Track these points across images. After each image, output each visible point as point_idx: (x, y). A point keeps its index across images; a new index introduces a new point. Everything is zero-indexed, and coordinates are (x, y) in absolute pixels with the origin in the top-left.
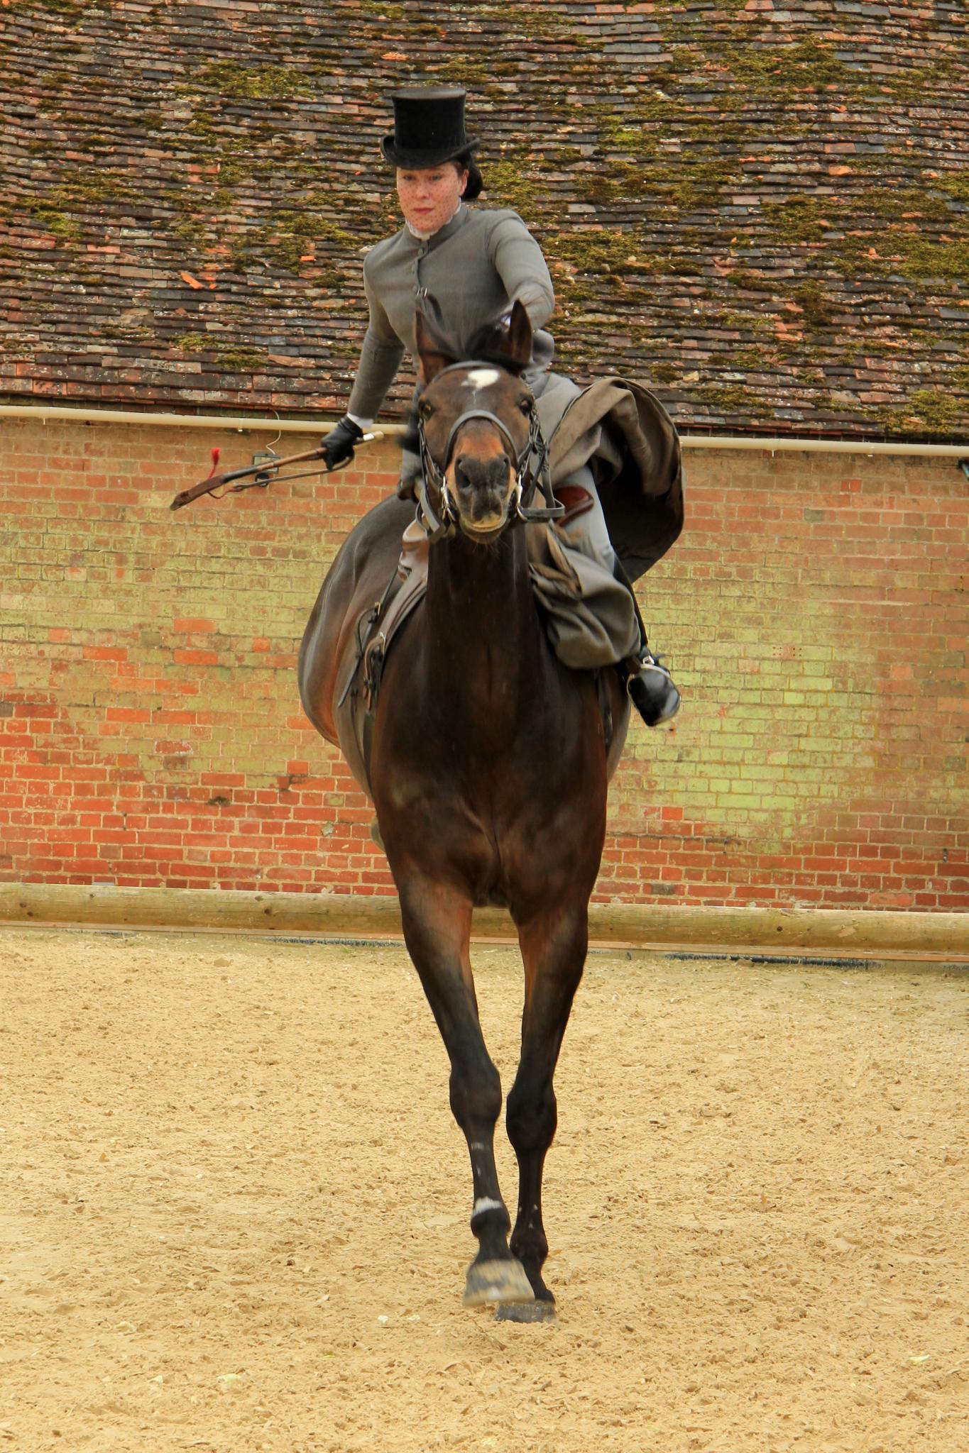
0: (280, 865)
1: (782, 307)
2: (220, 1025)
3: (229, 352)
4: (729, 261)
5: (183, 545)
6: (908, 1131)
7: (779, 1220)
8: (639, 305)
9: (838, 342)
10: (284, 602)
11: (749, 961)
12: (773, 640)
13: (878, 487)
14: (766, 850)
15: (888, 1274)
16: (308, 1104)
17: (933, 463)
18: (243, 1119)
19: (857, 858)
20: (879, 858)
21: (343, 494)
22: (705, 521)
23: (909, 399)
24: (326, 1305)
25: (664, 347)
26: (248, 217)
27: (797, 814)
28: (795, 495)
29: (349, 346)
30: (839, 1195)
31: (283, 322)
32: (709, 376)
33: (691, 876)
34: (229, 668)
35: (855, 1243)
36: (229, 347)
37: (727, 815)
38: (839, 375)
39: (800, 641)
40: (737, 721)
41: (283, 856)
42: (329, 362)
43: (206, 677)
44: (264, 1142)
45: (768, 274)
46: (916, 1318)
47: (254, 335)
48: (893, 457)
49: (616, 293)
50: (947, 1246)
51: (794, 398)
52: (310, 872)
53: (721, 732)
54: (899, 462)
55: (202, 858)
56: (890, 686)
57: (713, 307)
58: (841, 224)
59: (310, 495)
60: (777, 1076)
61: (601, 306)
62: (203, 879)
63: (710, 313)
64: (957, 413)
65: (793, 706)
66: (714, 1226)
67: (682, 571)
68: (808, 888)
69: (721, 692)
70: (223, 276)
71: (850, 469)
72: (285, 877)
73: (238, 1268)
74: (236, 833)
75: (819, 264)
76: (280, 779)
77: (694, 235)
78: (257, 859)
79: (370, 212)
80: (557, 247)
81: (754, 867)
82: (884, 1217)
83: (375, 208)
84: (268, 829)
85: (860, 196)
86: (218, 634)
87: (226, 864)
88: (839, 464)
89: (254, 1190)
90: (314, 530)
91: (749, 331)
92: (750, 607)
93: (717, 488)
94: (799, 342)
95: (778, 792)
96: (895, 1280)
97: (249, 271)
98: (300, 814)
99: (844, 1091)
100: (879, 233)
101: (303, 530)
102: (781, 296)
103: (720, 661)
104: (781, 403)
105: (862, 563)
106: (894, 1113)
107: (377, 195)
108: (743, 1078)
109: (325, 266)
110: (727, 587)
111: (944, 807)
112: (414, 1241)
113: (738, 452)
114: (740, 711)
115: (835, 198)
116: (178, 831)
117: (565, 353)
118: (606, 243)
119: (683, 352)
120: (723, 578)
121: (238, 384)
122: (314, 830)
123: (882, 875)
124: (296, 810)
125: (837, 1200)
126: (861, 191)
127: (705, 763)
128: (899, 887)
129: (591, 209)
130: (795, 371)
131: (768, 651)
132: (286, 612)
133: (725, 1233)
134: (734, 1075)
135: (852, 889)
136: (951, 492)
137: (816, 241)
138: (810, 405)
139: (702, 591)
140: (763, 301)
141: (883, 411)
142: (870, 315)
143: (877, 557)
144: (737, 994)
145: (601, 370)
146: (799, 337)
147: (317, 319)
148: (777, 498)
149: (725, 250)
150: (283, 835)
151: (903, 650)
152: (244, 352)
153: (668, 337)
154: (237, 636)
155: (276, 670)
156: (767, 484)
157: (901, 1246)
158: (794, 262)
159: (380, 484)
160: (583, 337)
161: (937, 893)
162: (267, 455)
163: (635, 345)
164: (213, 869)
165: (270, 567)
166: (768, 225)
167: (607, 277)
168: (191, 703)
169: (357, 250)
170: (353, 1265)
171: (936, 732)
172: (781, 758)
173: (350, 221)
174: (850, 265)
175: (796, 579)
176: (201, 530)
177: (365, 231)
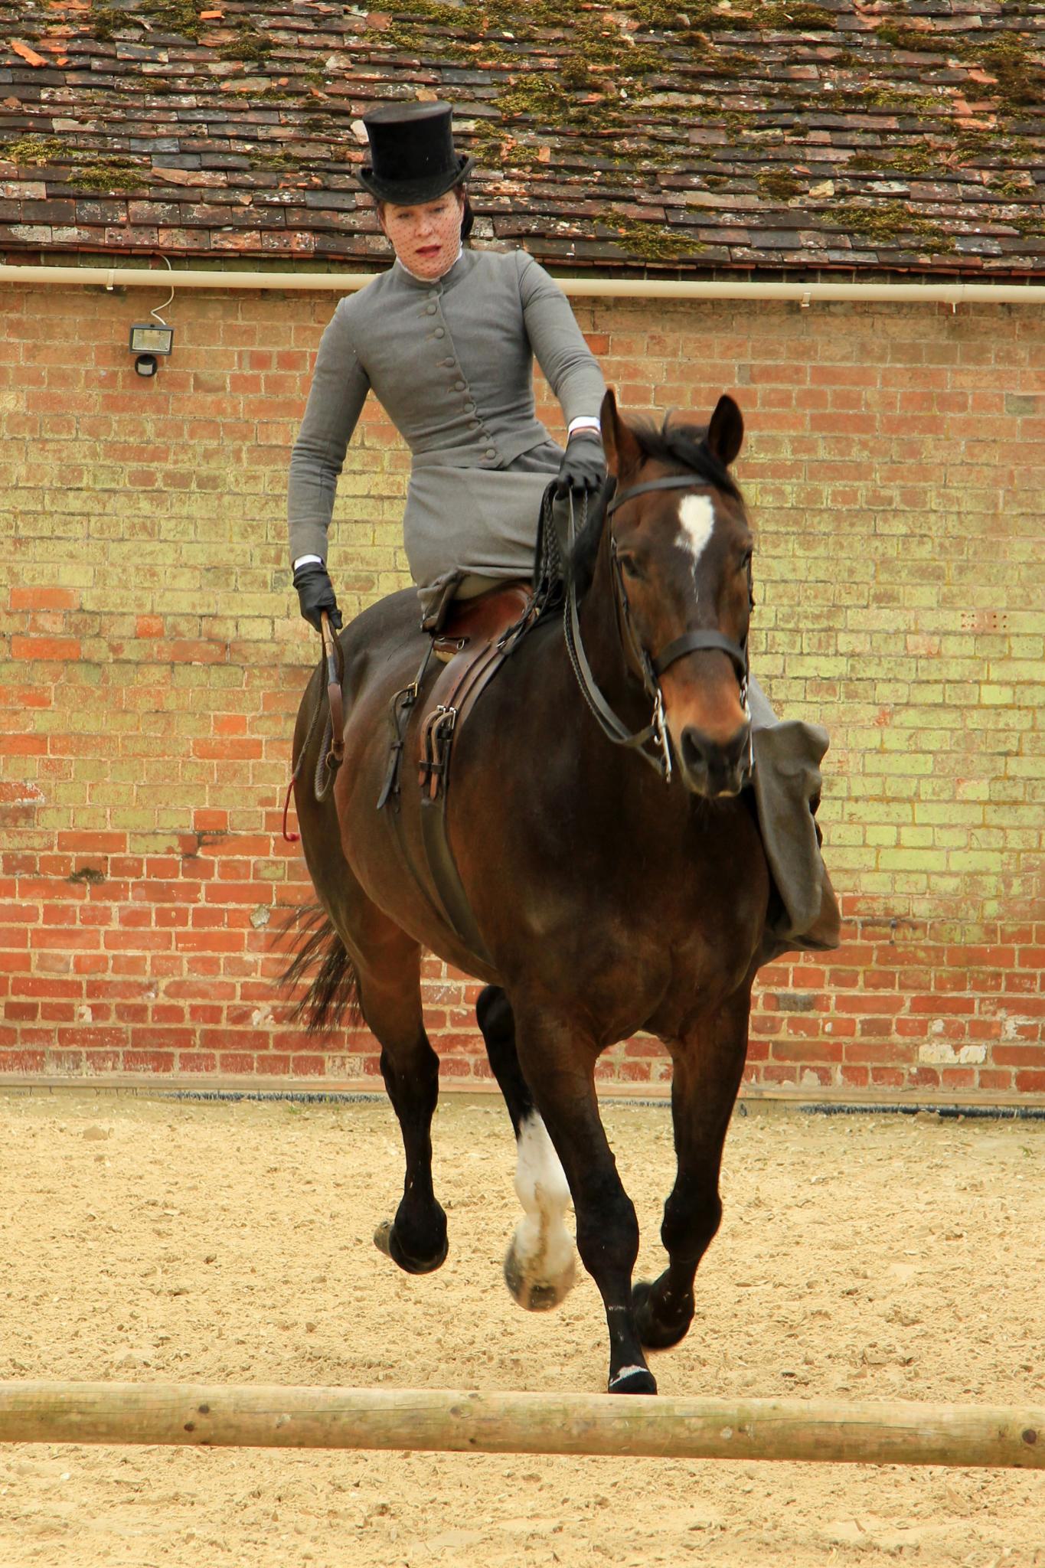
1: (964, 76)
2: (94, 1233)
3: (89, 164)
5: (23, 470)
7: (993, 1529)
8: (737, 79)
10: (183, 560)
11: (935, 1115)
12: (963, 604)
14: (957, 938)
21: (275, 385)
22: (848, 417)
25: (779, 143)
27: (1006, 880)
28: (992, 372)
31: (174, 116)
32: (850, 188)
33: (839, 980)
34: (99, 665)
36: (89, 156)
37: (894, 882)
39: (1004, 604)
40: (909, 732)
41: (191, 961)
42: (249, 178)
43: (62, 679)
45: (941, 25)
47: (130, 137)
49: (700, 60)
51: (985, 219)
52: (234, 986)
53: (881, 751)
55: (61, 966)
57: (854, 79)
59: (224, 388)
60: (984, 1298)
61: (677, 80)
62: (64, 1000)
63: (849, 87)
65: (996, 707)
66: (890, 1541)
67: (814, 496)
68: (1025, 995)
69: (880, 686)
70: (77, 45)
72: (193, 995)
74: (115, 926)
76: (184, 839)
78: (148, 968)
81: (941, 964)
86: (81, 610)
87: (99, 977)
90: (230, 444)
91: (912, 115)
92: (924, 552)
93: (867, 364)
94: (992, 131)
95: (975, 845)
97: (119, 35)
98: (214, 894)
101: (213, 444)
102: (962, 60)
103: (878, 639)
104: (965, 228)
108: (929, 1302)
109: (239, 25)
110: (885, 520)
113: (899, 307)
114: (910, 717)
116: (22, 925)
117: (622, 156)
119: (807, 151)
120: (880, 507)
121: (104, 215)
122: (244, 919)
124: (208, 887)
127: (857, 800)
130: (986, 176)
131: (952, 620)
133: (906, 1551)
134: (915, 1296)
138: (1010, 230)
139: (845, 527)
140: (935, 67)
144: (920, 1168)
145: (679, 182)
146: (992, 123)
147: (228, 110)
148: (962, 378)
150: (189, 928)
152: (113, 164)
153: (784, 127)
154: (111, 613)
155: (173, 665)
156: (944, 355)
160: (650, 130)
162: (152, 327)
163: (732, 142)
164: (79, 985)
165: (160, 503)
167: (686, 34)
168: (40, 722)
172: (978, 789)
175: (996, 506)
176: (50, 446)
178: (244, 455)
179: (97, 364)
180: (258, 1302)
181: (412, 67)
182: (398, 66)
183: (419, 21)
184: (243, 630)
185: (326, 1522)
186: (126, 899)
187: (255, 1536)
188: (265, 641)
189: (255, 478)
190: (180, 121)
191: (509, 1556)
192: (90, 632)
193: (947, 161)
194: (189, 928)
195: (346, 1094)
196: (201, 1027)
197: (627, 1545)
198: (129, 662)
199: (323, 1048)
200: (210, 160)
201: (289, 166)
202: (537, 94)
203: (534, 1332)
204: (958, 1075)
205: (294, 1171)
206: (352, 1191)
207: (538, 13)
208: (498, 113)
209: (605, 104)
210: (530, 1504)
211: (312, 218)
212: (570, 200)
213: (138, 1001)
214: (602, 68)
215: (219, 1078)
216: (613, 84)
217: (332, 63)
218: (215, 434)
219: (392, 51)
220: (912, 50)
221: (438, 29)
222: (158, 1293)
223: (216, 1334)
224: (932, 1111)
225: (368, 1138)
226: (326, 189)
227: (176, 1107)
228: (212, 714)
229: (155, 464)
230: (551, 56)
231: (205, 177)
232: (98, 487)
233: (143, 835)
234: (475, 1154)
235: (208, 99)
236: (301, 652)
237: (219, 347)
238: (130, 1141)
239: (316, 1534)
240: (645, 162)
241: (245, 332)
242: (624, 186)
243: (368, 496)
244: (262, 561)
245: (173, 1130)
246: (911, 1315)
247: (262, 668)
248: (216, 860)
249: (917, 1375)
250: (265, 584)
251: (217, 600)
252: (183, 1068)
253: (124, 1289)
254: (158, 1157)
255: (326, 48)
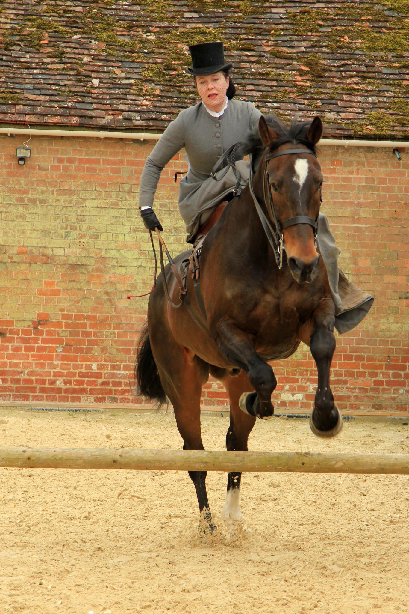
0: (34, 369)
1: (299, 67)
4: (270, 43)
6: (370, 507)
9: (328, 86)
10: (34, 228)
11: (286, 417)
13: (350, 164)
15: (361, 584)
16: (50, 497)
17: (379, 151)
18: (15, 505)
19: (342, 361)
20: (354, 361)
21: (66, 169)
23: (366, 116)
24: (60, 606)
26: (11, 19)
29: (67, 89)
30: (334, 542)
31: (31, 77)
32: (260, 105)
34: (5, 263)
35: (343, 567)
38: (329, 104)
41: (36, 364)
42: (57, 98)
44: (26, 518)
45: (291, 50)
46: (375, 607)
47: (16, 83)
48: (358, 148)
50: (391, 568)
52: (50, 373)
54: (361, 150)
56: (358, 270)
57: (262, 68)
58: (329, 23)
59: (48, 170)
63: (260, 71)
64: (392, 124)
66: (268, 560)
71: (336, 154)
72: (37, 375)
73: (13, 587)
74: (10, 352)
75: (318, 44)
76: (33, 322)
77: (251, 29)
78: (21, 366)
79: (78, 17)
80: (178, 36)
81: (288, 366)
82: (358, 553)
83: (80, 15)
84: (27, 349)
85: (339, 8)
88: (330, 152)
89: (21, 544)
90: (50, 189)
91: (281, 81)
94: (308, 86)
96: (364, 587)
97: (12, 48)
98: (44, 341)
99: (337, 486)
100: (350, 28)
102: (298, 62)
105: (343, 204)
106: (363, 497)
107: (81, 8)
108: (283, 480)
109: (54, 46)
111: (388, 334)
112: (108, 570)
115: (326, 9)
117: (183, 93)
118: (204, 33)
119: (246, 92)
122: (54, 350)
123: (355, 370)
125: (333, 544)
126: (339, 6)
128: (365, 376)
129: (196, 15)
130: (306, 102)
132: (36, 232)
133: (274, 563)
135: (340, 378)
136: (389, 166)
137: (316, 32)
140: (288, 64)
141: (353, 123)
142: (345, 71)
143: (351, 201)
144: (280, 435)
146: (308, 84)
147: (50, 75)
149: (268, 37)
150: (35, 353)
151: (364, 250)
152: (11, 92)
154: (9, 246)
155: (30, 263)
157: (367, 568)
158: (304, 44)
159: (86, 163)
161: (385, 380)
162: (24, 148)
165: (26, 208)
166: (291, 24)
169: (70, 37)
170: (75, 584)
171: (383, 294)
173: (66, 21)
174: (334, 45)
177: (75, 27)
178: (55, 193)
179: (5, 160)
180: (58, 479)
181: (113, 61)
182: (108, 61)
183: (115, 45)
184: (54, 252)
185: (80, 553)
186: (14, 342)
187: (55, 558)
188: (62, 256)
189: (59, 200)
190: (33, 78)
191: (141, 565)
192: (2, 252)
193: (293, 96)
194: (35, 353)
195: (88, 409)
196: (39, 386)
197: (181, 561)
198: (15, 262)
199: (81, 394)
200: (43, 92)
201: (71, 94)
202: (155, 71)
203: (151, 489)
204: (293, 403)
205: (70, 435)
206: (90, 442)
207: (155, 43)
208: (142, 77)
209: (178, 75)
210: (148, 547)
211: (78, 112)
212: (166, 107)
213: (18, 377)
214: (177, 63)
215: (45, 403)
216: (181, 68)
217: (86, 59)
218: (45, 185)
219: (106, 55)
220: (281, 58)
221: (121, 49)
222: (24, 476)
223: (43, 490)
224: (285, 416)
225: (96, 424)
226: (83, 102)
227: (30, 413)
228: (44, 280)
229: (24, 195)
230: (160, 58)
231: (42, 98)
232: (5, 203)
233: (20, 321)
234: (131, 430)
235: (43, 71)
236: (74, 260)
237: (46, 156)
238: (14, 424)
239: (76, 557)
240: (192, 95)
241: (56, 151)
242: (185, 103)
243: (97, 207)
244: (61, 228)
245: (29, 421)
246: (277, 484)
247: (61, 265)
248: (45, 330)
249: (278, 504)
250: (62, 236)
251: (45, 242)
252: (33, 400)
253: (12, 475)
254: (24, 430)
255: (83, 54)
